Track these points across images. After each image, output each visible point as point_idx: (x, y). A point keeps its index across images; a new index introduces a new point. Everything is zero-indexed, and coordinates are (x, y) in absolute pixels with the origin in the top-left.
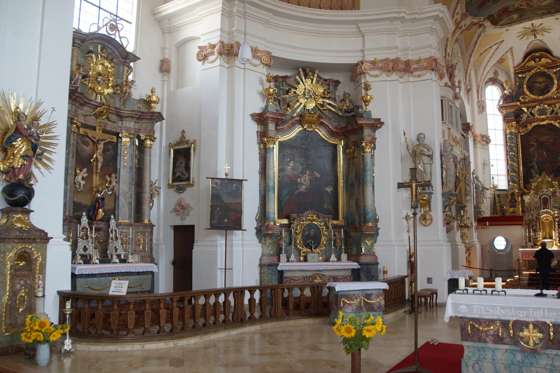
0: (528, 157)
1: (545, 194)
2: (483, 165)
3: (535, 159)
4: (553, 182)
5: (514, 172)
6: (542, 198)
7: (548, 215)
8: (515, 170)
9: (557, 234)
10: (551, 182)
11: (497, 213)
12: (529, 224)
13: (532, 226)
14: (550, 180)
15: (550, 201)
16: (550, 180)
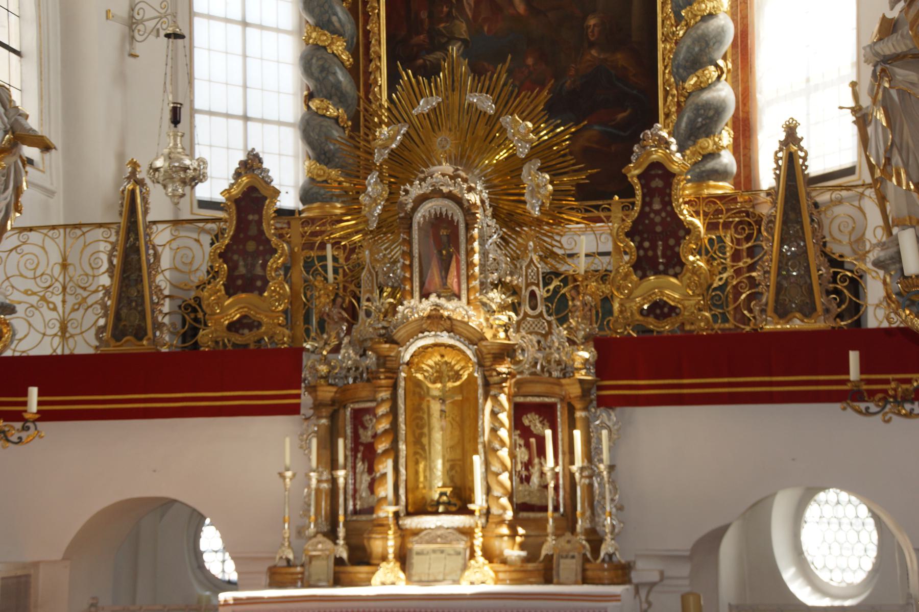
0: (424, 15)
1: (437, 193)
2: (116, 30)
3: (462, 28)
4: (506, 120)
5: (329, 97)
6: (418, 217)
7: (445, 338)
8: (337, 86)
9: (505, 478)
10: (492, 121)
11: (140, 334)
12: (334, 409)
13: (358, 415)
14: (488, 105)
15: (470, 240)
16: (488, 105)
